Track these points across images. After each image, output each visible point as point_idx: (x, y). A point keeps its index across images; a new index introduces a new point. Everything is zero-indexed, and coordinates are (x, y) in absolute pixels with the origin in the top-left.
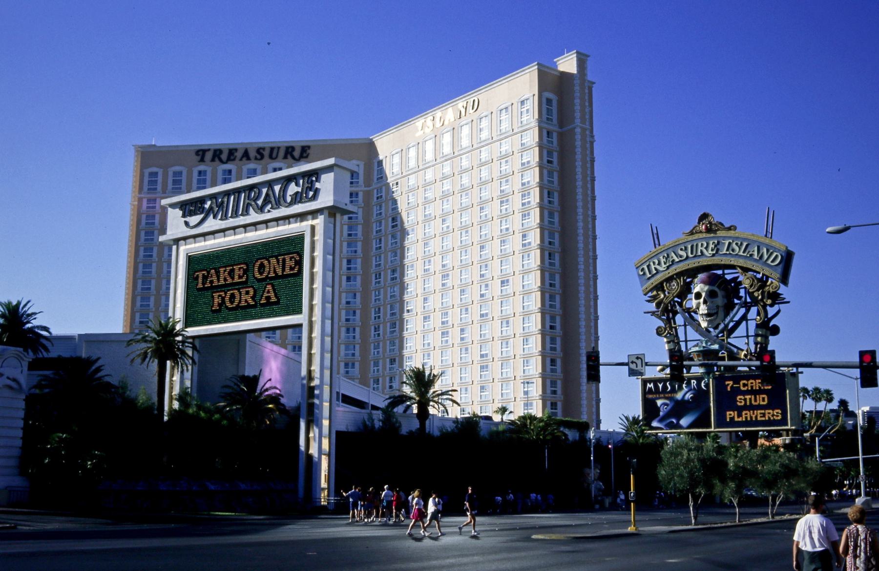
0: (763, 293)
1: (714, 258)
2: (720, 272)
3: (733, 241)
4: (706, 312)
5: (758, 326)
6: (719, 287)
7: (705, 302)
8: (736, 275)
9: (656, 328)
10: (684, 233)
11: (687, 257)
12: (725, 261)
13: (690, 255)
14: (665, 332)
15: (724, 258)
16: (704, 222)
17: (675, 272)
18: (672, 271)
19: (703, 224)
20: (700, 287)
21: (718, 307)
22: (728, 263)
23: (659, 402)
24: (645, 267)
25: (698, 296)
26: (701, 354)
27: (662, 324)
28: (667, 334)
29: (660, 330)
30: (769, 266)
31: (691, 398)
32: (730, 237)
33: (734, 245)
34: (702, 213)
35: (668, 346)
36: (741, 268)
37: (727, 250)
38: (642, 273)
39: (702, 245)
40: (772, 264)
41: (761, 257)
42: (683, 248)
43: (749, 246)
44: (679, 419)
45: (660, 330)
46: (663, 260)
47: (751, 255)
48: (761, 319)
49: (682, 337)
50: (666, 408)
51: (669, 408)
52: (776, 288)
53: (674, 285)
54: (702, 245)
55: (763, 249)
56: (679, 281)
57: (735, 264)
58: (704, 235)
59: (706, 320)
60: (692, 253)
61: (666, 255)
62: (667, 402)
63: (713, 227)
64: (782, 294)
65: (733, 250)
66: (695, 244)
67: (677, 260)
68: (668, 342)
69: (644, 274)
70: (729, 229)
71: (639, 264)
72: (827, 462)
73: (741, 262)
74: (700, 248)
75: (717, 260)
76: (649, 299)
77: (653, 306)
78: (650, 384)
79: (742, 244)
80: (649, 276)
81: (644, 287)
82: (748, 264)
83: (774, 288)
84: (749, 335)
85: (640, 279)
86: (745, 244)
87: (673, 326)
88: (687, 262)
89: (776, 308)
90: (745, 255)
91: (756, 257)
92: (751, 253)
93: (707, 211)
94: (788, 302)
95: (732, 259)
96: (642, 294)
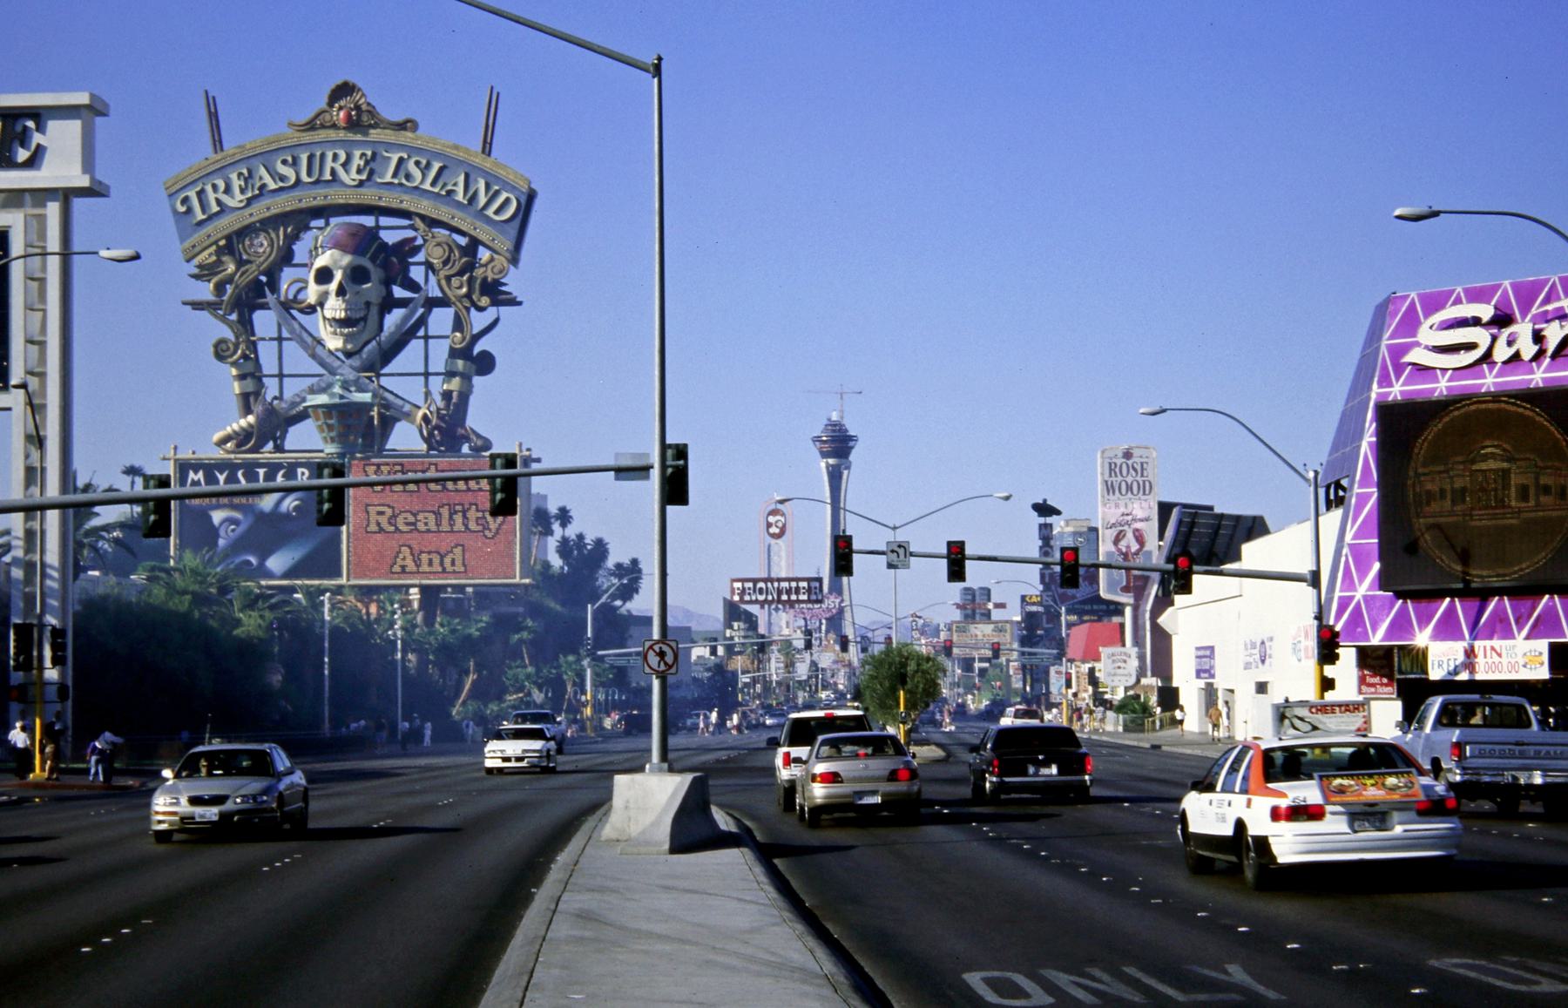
0: (471, 281)
3: (409, 157)
4: (343, 315)
5: (454, 353)
6: (373, 259)
7: (341, 292)
8: (410, 234)
9: (214, 341)
10: (291, 124)
11: (298, 182)
12: (389, 199)
13: (305, 178)
14: (235, 352)
15: (384, 193)
16: (342, 103)
17: (267, 214)
18: (260, 211)
19: (341, 108)
20: (332, 255)
21: (368, 304)
22: (395, 205)
23: (217, 516)
24: (192, 194)
25: (324, 276)
26: (334, 413)
27: (229, 334)
28: (239, 359)
29: (224, 346)
30: (489, 220)
31: (296, 508)
32: (401, 147)
35: (240, 387)
36: (423, 218)
37: (395, 175)
38: (182, 209)
39: (335, 157)
40: (497, 218)
41: (473, 199)
42: (290, 159)
43: (446, 172)
44: (263, 558)
45: (224, 346)
46: (236, 183)
47: (450, 193)
48: (464, 339)
49: (268, 364)
50: (233, 530)
51: (241, 529)
52: (501, 272)
53: (262, 245)
54: (335, 157)
55: (476, 181)
56: (273, 235)
57: (412, 209)
58: (342, 135)
59: (342, 334)
60: (309, 174)
61: (245, 172)
62: (237, 515)
63: (365, 118)
64: (505, 284)
65: (408, 177)
66: (318, 154)
67: (272, 186)
68: (242, 377)
69: (189, 211)
70: (402, 126)
71: (178, 187)
72: (609, 655)
73: (425, 207)
74: (329, 164)
75: (368, 196)
76: (196, 271)
77: (206, 291)
78: (196, 472)
79: (428, 165)
80: (200, 216)
81: (187, 244)
82: (442, 212)
83: (496, 270)
84: (431, 370)
85: (177, 222)
86: (436, 166)
87: (252, 338)
88: (297, 193)
89: (491, 313)
91: (460, 197)
92: (449, 188)
93: (352, 79)
95: (405, 197)
96: (180, 257)
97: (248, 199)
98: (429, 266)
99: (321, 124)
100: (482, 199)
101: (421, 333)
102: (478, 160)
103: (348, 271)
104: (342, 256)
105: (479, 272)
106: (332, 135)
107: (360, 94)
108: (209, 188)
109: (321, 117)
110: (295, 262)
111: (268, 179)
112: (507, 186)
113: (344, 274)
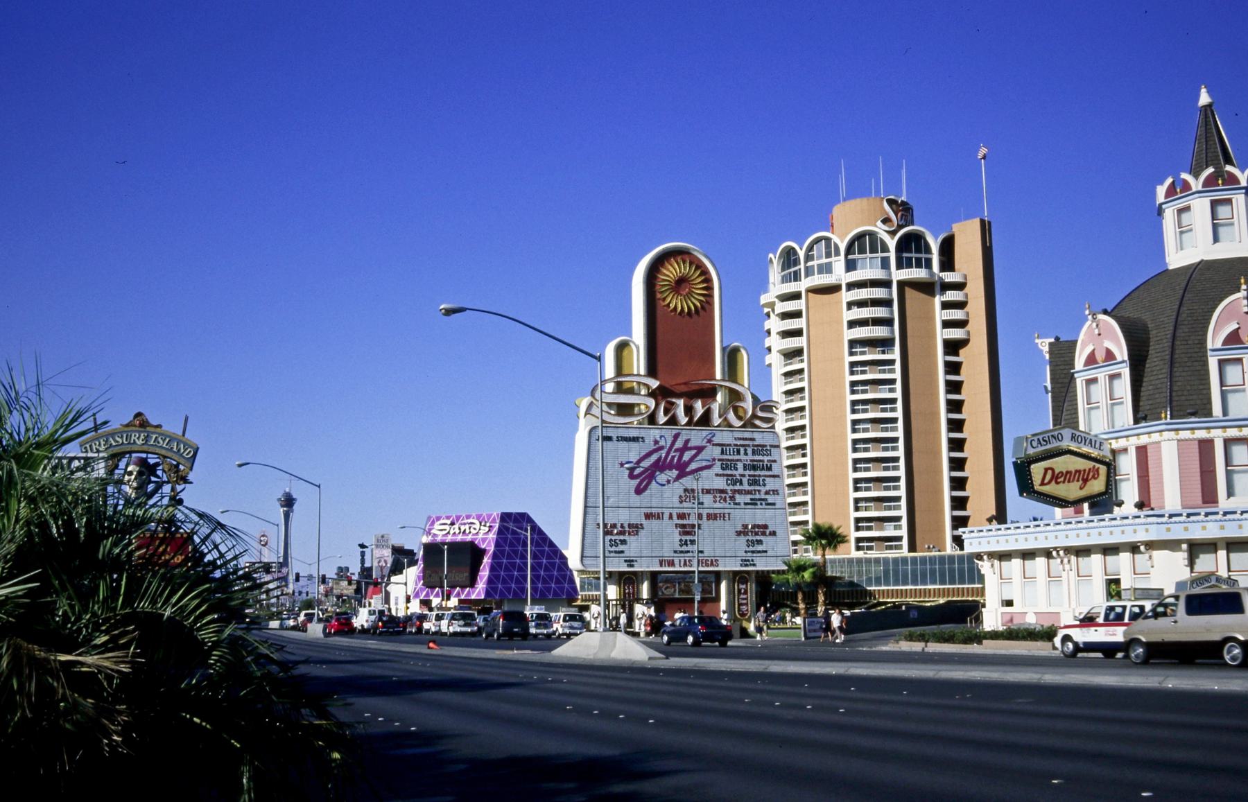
0: (177, 476)
1: (143, 446)
2: (144, 455)
7: (135, 479)
8: (158, 460)
10: (121, 425)
11: (123, 443)
13: (125, 442)
24: (88, 446)
30: (184, 457)
33: (160, 439)
37: (154, 442)
41: (179, 450)
46: (102, 443)
47: (172, 448)
54: (135, 436)
58: (137, 429)
60: (126, 440)
65: (158, 442)
67: (114, 444)
73: (163, 452)
75: (145, 448)
79: (165, 439)
82: (169, 454)
86: (168, 440)
88: (123, 447)
90: (167, 447)
91: (175, 449)
94: (191, 483)
95: (157, 449)
98: (164, 471)
101: (160, 492)
102: (181, 438)
105: (180, 473)
106: (134, 428)
108: (93, 444)
110: (119, 468)
111: (113, 442)
112: (191, 447)
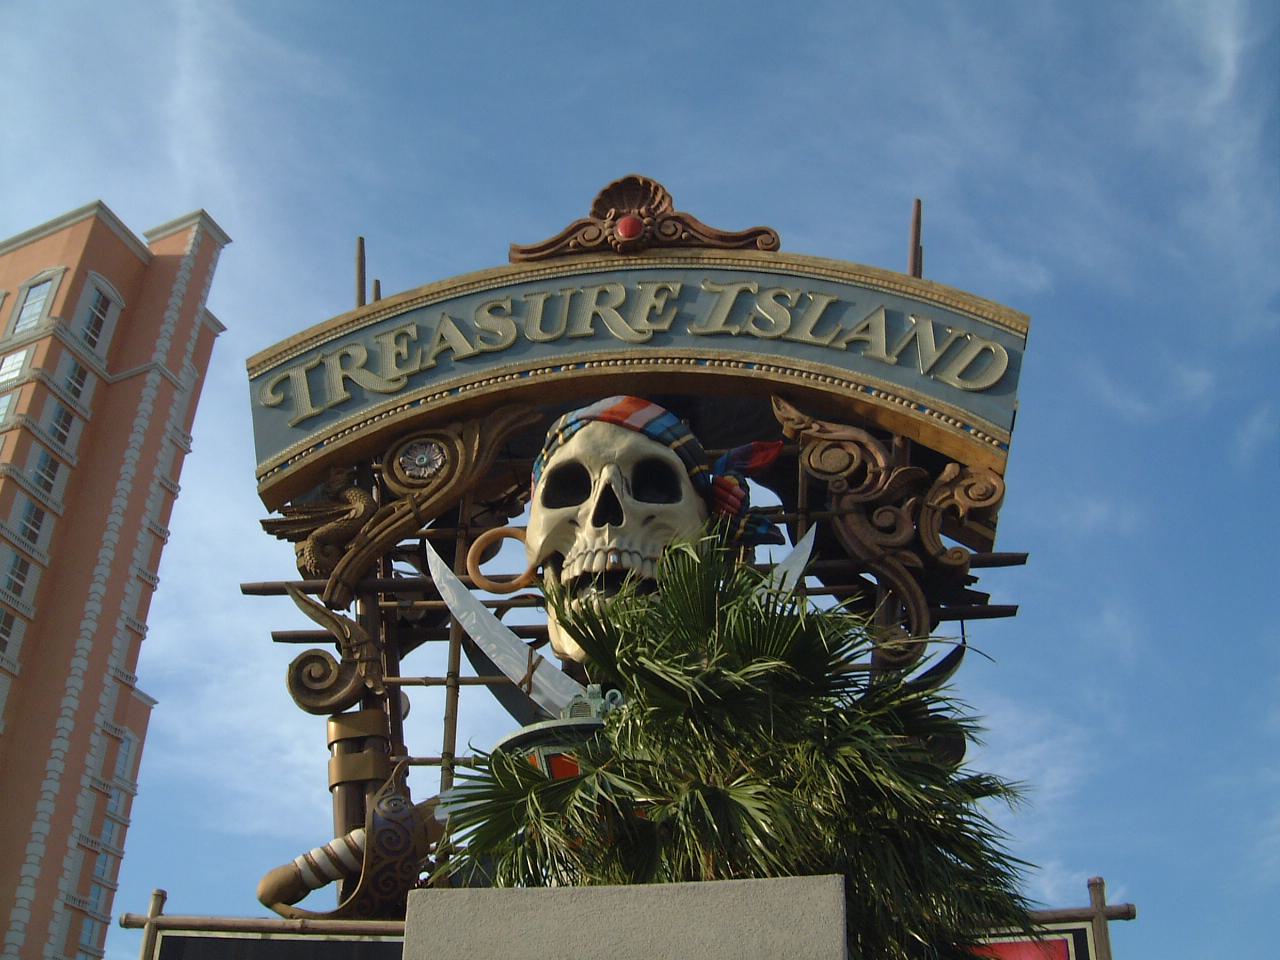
7: (608, 513)
13: (535, 332)
14: (340, 682)
15: (711, 351)
18: (434, 395)
20: (589, 435)
24: (298, 375)
29: (316, 669)
30: (948, 392)
34: (619, 176)
41: (906, 357)
42: (507, 306)
45: (316, 669)
56: (459, 446)
60: (545, 326)
67: (464, 348)
69: (285, 404)
74: (590, 305)
80: (306, 408)
81: (269, 462)
88: (514, 363)
90: (826, 341)
92: (854, 336)
97: (410, 376)
99: (576, 246)
100: (929, 351)
103: (628, 474)
104: (613, 436)
107: (660, 194)
108: (334, 363)
109: (579, 234)
113: (618, 472)
